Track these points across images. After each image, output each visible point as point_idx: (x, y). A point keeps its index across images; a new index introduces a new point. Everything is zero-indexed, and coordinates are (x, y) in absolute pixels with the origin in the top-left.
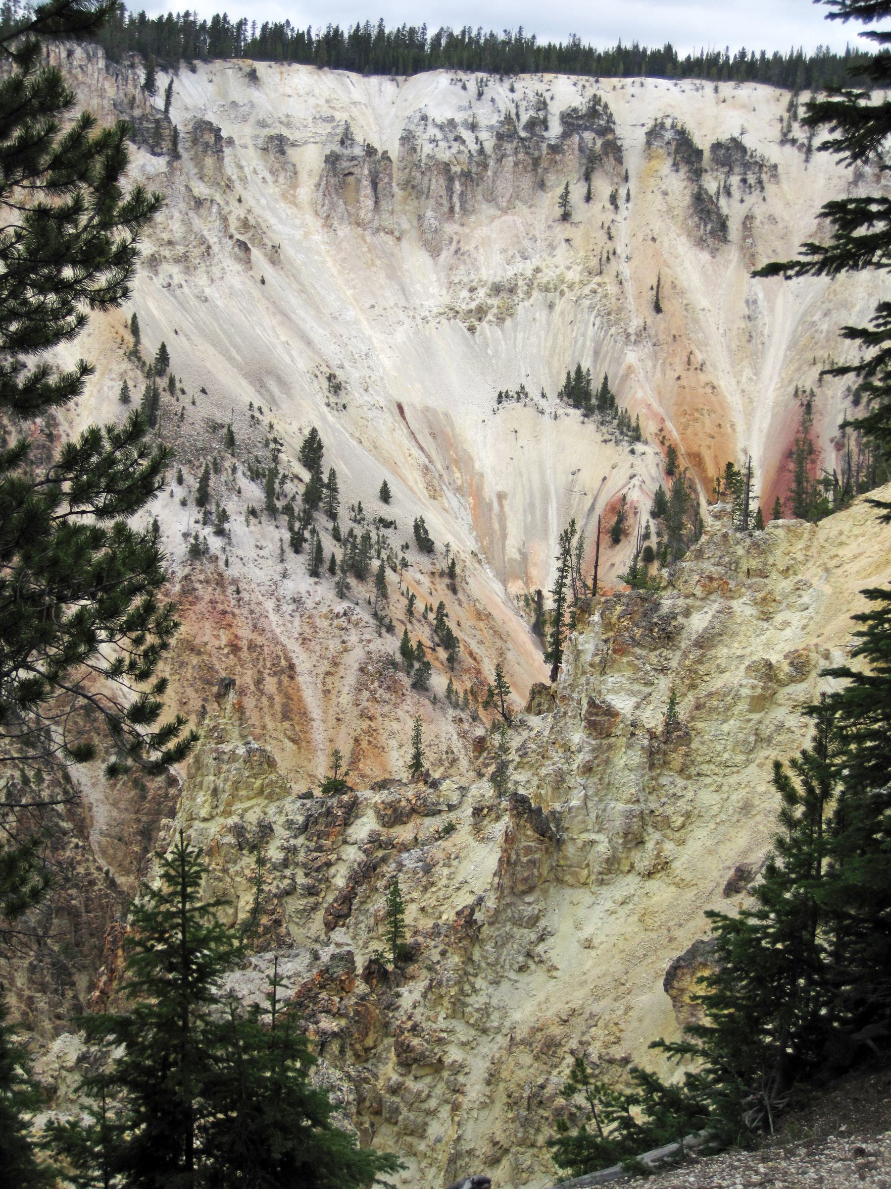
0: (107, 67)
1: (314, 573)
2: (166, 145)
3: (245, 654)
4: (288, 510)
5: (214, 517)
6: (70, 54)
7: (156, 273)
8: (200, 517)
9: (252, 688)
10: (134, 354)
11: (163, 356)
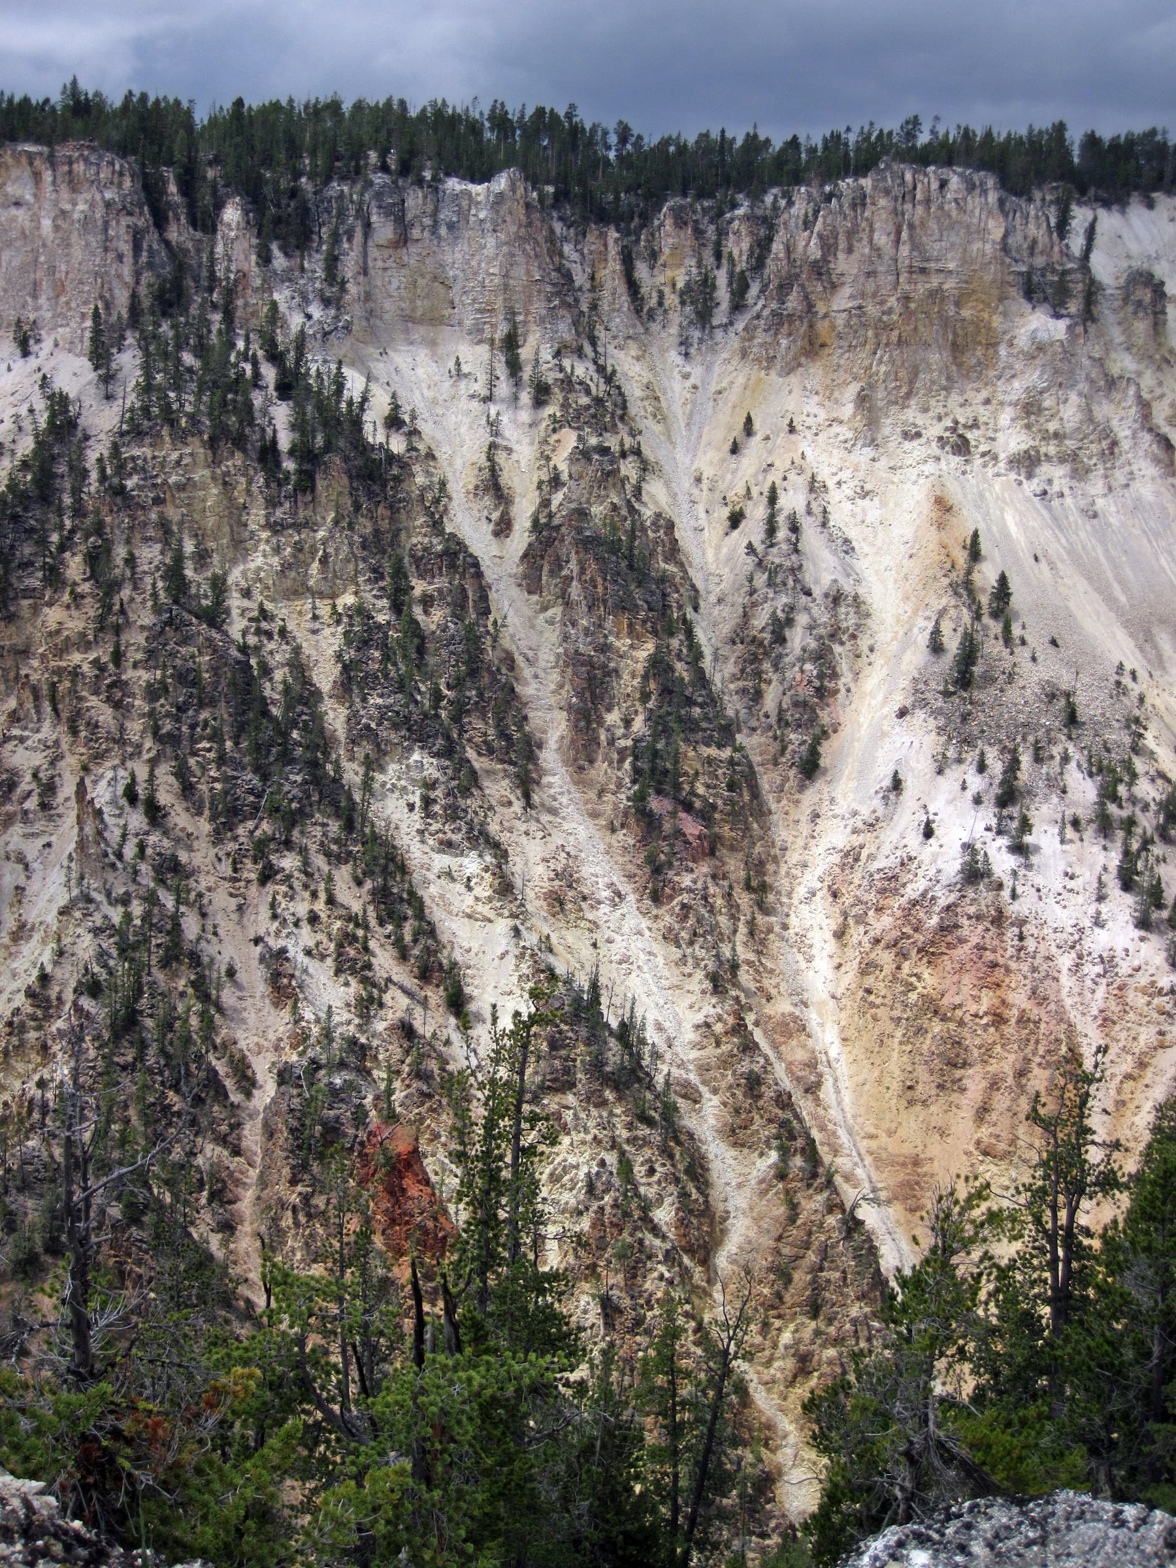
0: (1001, 202)
1: (1143, 923)
2: (1074, 306)
3: (1010, 1030)
4: (1129, 824)
5: (1015, 825)
6: (943, 184)
7: (1030, 476)
8: (993, 822)
9: (1010, 1080)
10: (965, 588)
11: (1003, 591)
